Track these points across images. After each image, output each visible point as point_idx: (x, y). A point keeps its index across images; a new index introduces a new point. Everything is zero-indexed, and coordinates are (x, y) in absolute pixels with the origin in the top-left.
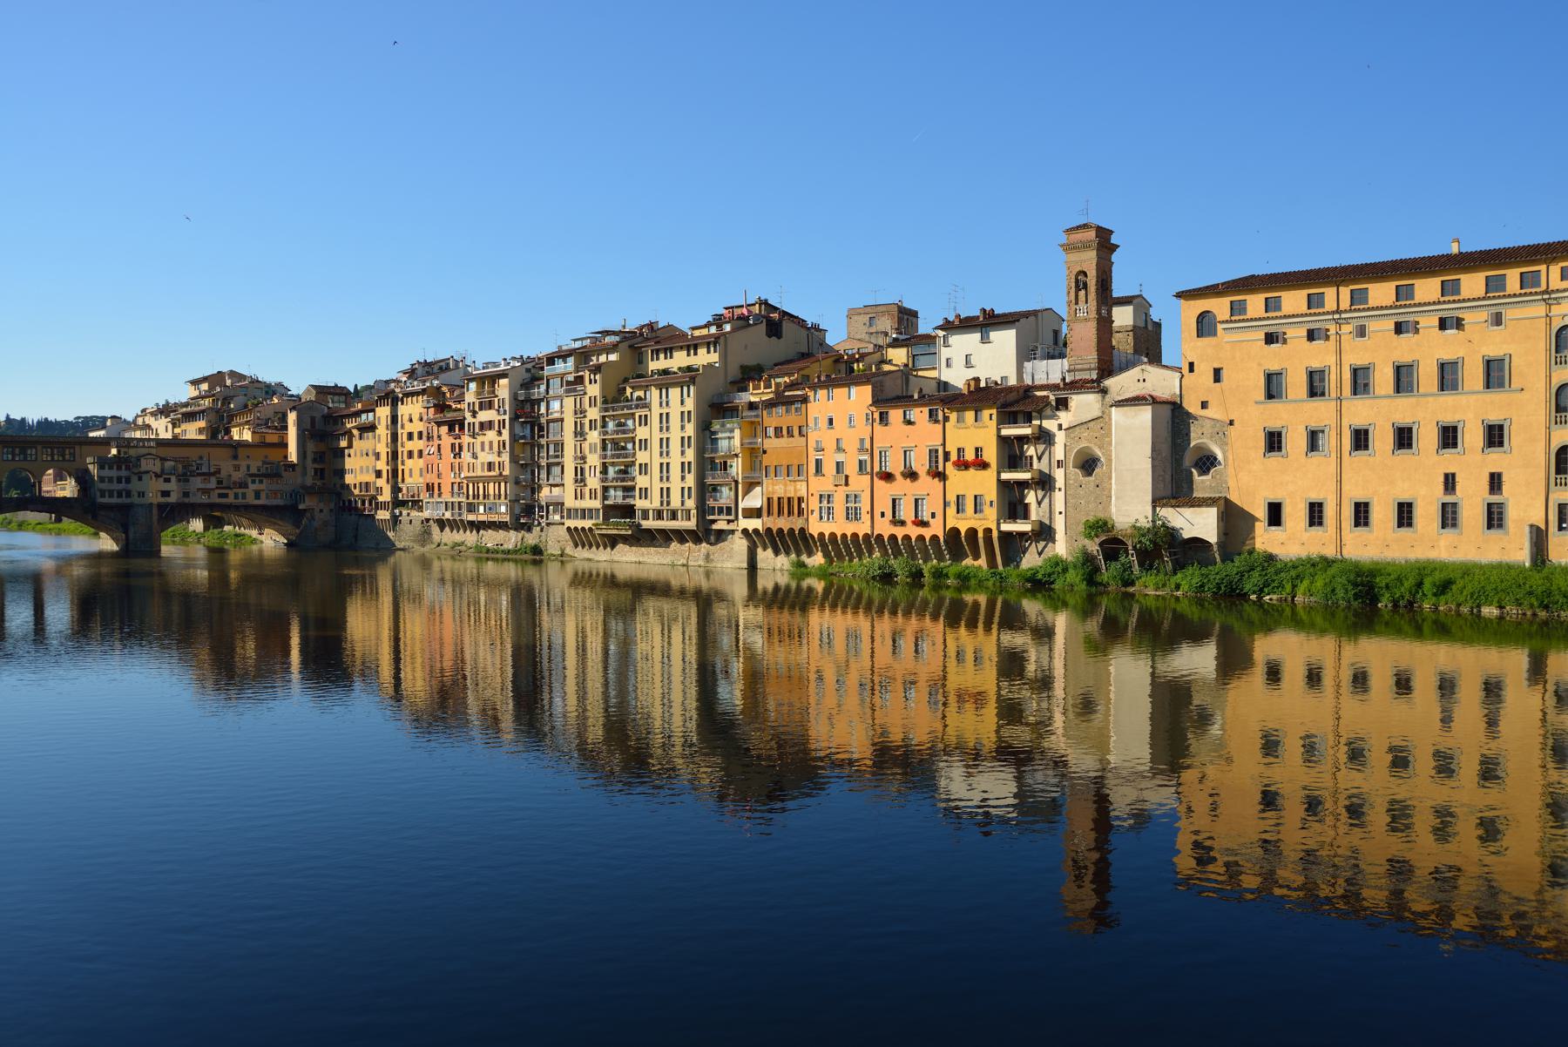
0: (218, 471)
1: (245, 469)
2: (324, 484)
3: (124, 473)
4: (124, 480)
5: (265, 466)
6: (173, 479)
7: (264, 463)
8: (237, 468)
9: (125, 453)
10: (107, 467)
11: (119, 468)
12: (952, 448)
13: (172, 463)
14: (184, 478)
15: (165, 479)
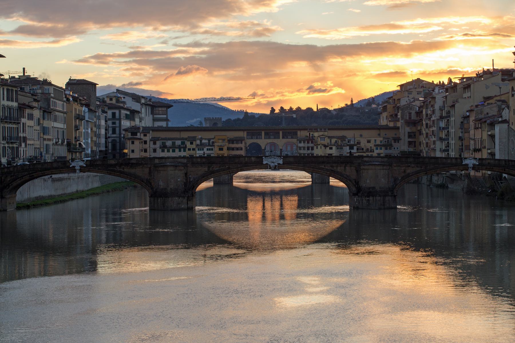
0: (359, 143)
1: (374, 142)
2: (415, 149)
3: (311, 145)
4: (310, 148)
5: (384, 140)
6: (334, 148)
7: (384, 138)
8: (369, 142)
9: (312, 134)
10: (302, 142)
11: (308, 143)
12: (483, 140)
13: (335, 139)
14: (340, 147)
15: (330, 148)
